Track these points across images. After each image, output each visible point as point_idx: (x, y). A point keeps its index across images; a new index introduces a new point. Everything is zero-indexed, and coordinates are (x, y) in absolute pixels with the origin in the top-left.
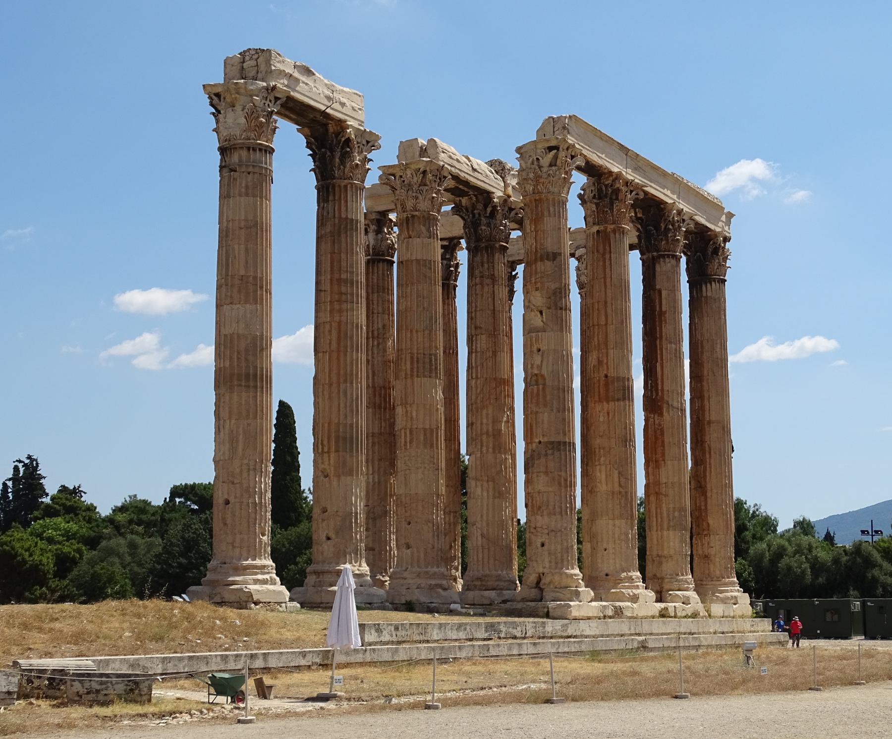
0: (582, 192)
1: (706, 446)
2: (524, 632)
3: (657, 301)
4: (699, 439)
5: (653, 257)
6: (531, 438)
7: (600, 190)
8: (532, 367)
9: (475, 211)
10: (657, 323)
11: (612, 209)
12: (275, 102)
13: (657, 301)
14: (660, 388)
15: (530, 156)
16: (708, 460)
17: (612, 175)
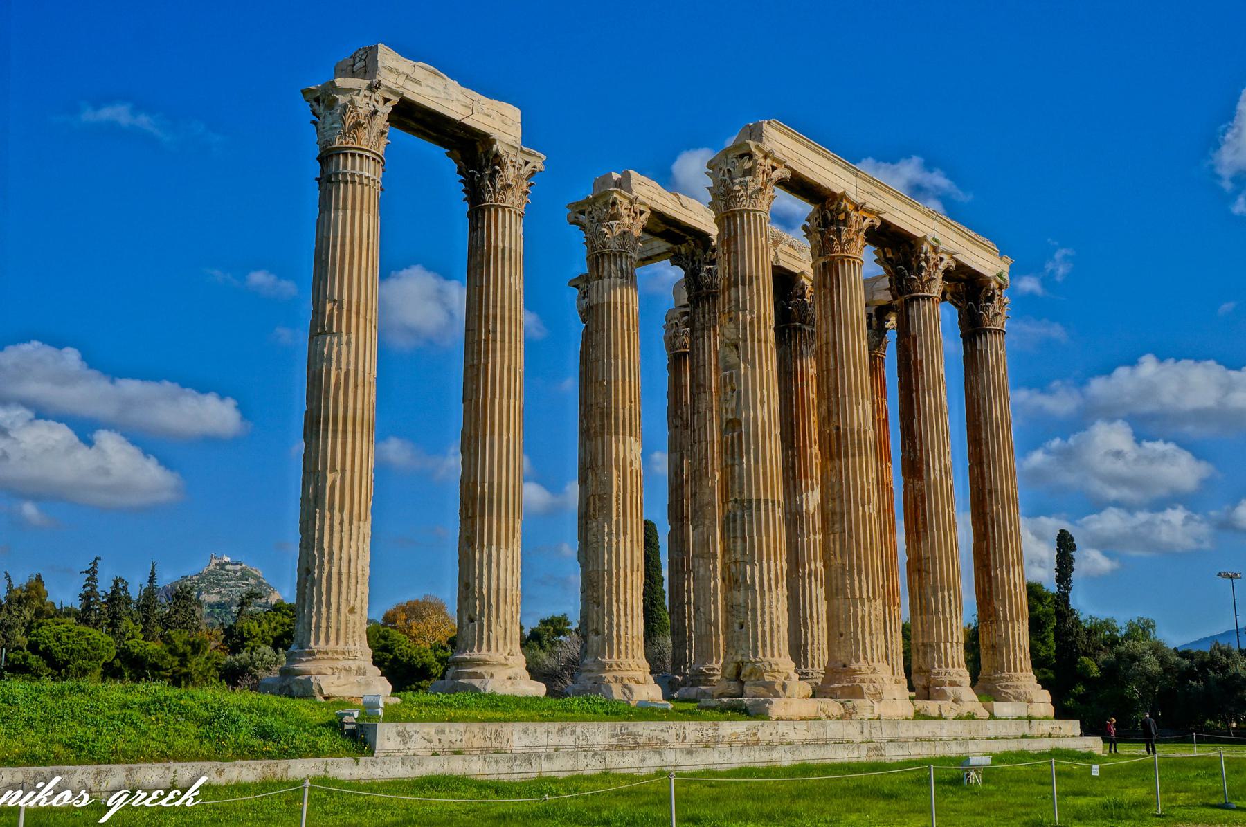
0: (808, 224)
1: (989, 518)
2: (682, 736)
3: (912, 349)
4: (981, 511)
5: (906, 300)
6: (727, 497)
7: (824, 217)
8: (727, 412)
9: (695, 258)
10: (913, 374)
11: (839, 237)
12: (385, 103)
13: (912, 349)
14: (918, 448)
15: (721, 169)
16: (991, 535)
17: (836, 198)
